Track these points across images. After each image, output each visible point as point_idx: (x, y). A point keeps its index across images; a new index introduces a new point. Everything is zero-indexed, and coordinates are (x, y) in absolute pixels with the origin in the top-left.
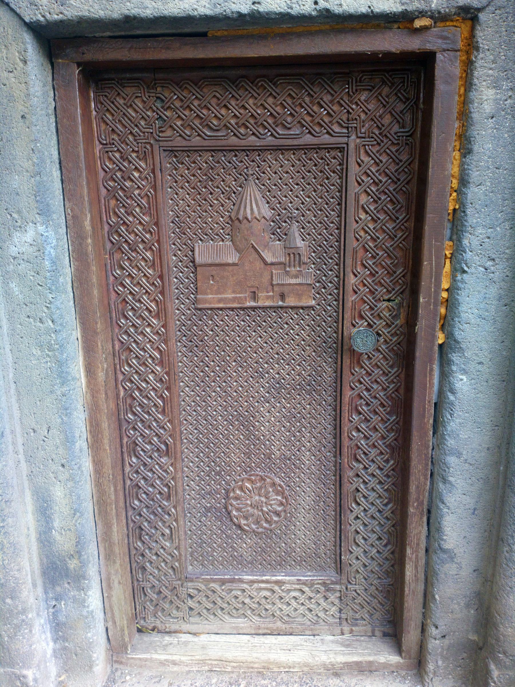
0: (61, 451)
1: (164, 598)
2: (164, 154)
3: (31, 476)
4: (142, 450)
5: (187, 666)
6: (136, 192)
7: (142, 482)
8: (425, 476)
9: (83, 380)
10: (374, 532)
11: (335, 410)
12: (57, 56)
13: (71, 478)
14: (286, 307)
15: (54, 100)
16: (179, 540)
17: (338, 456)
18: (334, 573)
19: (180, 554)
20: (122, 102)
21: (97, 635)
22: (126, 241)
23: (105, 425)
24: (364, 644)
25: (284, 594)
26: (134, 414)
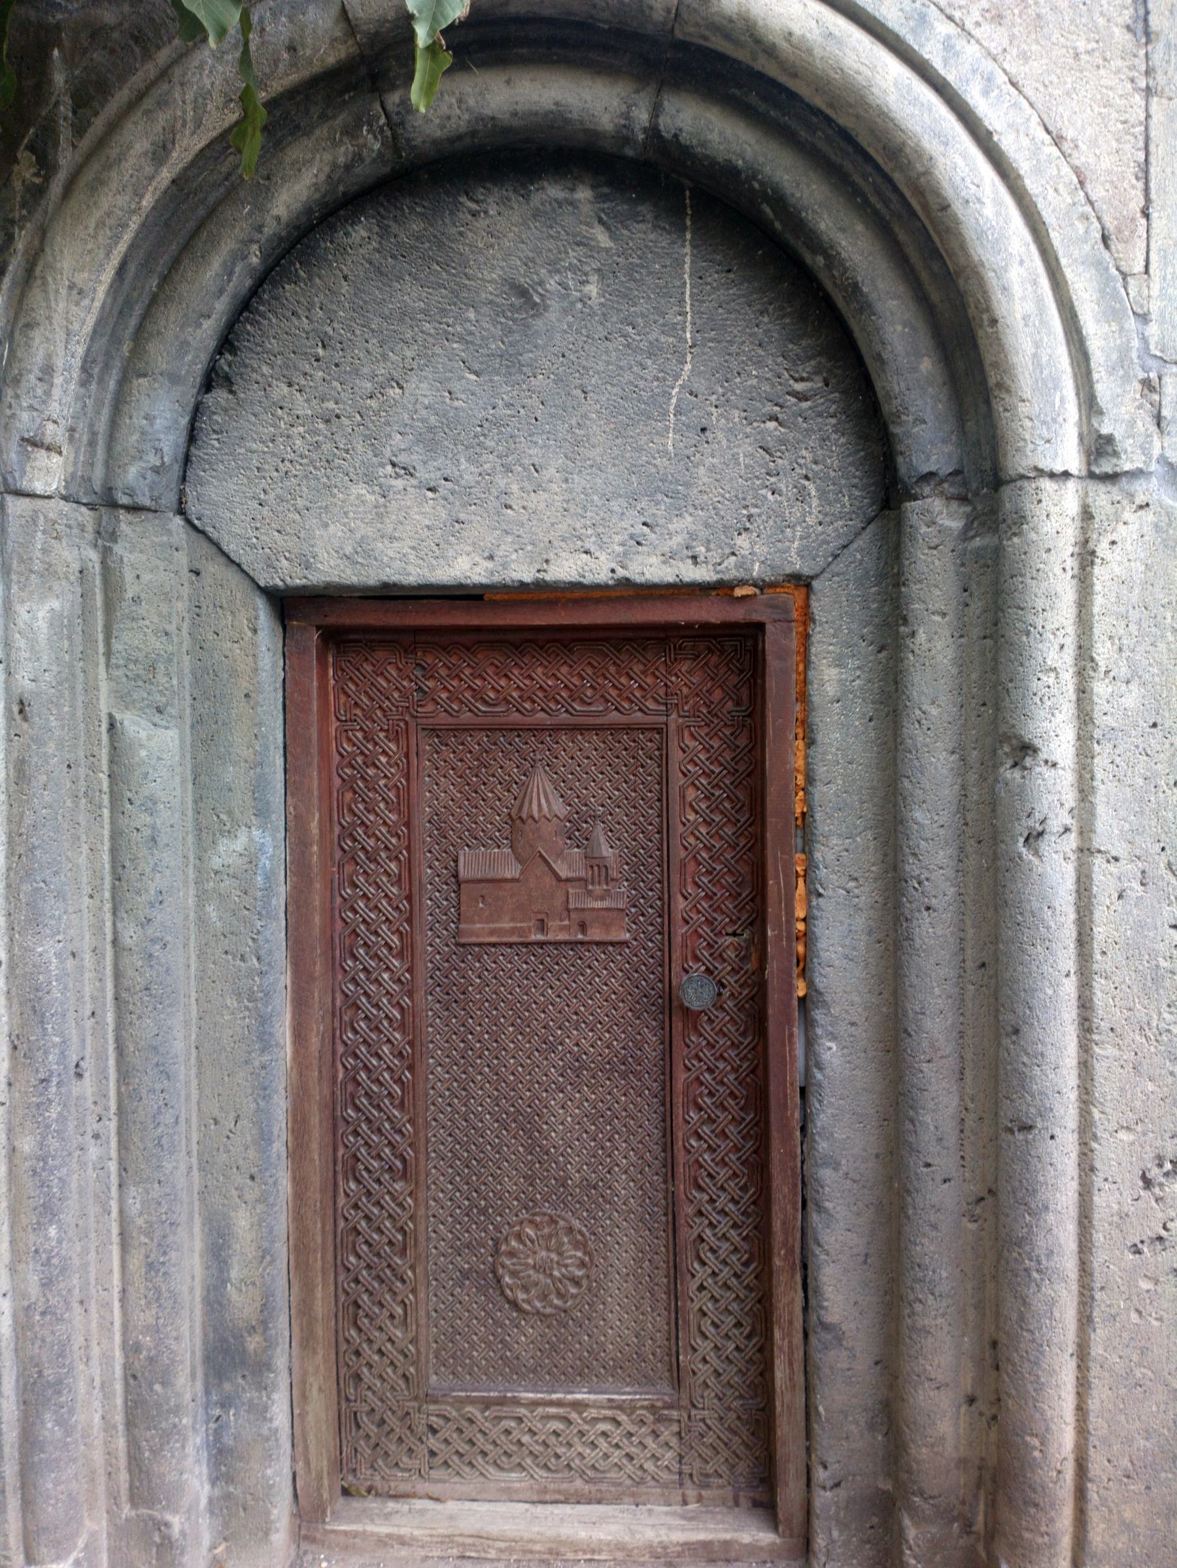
0: (252, 1153)
1: (388, 1433)
2: (422, 734)
3: (204, 1192)
4: (366, 1169)
6: (382, 782)
7: (363, 1223)
8: (794, 1204)
9: (289, 1049)
10: (730, 1313)
11: (663, 1105)
12: (291, 619)
13: (263, 1199)
14: (589, 943)
15: (284, 669)
16: (418, 1326)
17: (670, 1180)
18: (668, 1390)
20: (369, 668)
21: (278, 1473)
22: (363, 848)
23: (315, 1120)
24: (719, 1517)
25: (586, 1427)
26: (357, 1109)
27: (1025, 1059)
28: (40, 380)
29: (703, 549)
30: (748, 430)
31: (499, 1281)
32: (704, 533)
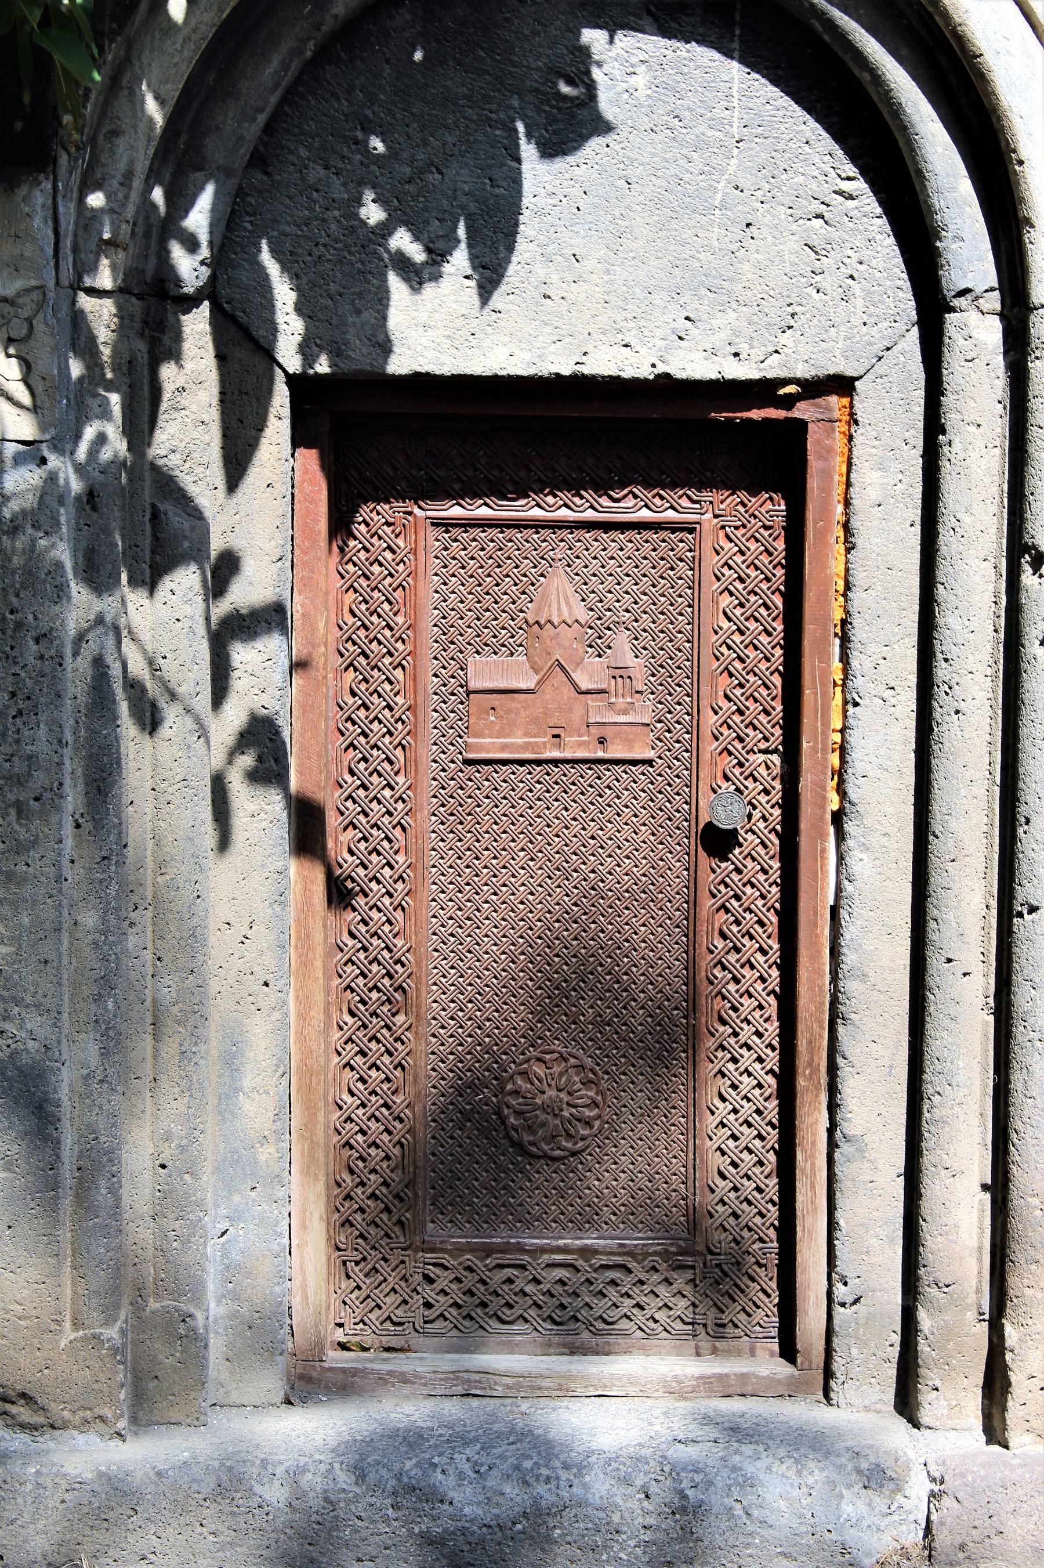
5: (425, 1385)
16: (416, 1167)
18: (685, 1235)
19: (416, 1194)
27: (1034, 846)
28: (122, 184)
29: (746, 346)
30: (794, 227)
31: (503, 1123)
32: (748, 331)
